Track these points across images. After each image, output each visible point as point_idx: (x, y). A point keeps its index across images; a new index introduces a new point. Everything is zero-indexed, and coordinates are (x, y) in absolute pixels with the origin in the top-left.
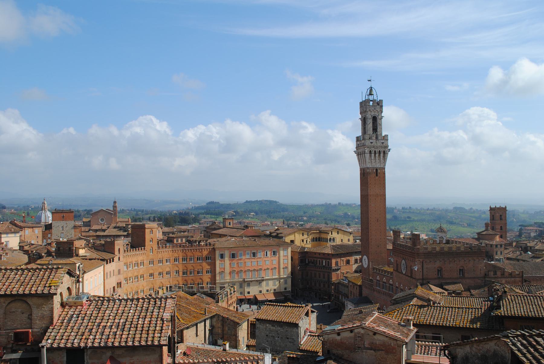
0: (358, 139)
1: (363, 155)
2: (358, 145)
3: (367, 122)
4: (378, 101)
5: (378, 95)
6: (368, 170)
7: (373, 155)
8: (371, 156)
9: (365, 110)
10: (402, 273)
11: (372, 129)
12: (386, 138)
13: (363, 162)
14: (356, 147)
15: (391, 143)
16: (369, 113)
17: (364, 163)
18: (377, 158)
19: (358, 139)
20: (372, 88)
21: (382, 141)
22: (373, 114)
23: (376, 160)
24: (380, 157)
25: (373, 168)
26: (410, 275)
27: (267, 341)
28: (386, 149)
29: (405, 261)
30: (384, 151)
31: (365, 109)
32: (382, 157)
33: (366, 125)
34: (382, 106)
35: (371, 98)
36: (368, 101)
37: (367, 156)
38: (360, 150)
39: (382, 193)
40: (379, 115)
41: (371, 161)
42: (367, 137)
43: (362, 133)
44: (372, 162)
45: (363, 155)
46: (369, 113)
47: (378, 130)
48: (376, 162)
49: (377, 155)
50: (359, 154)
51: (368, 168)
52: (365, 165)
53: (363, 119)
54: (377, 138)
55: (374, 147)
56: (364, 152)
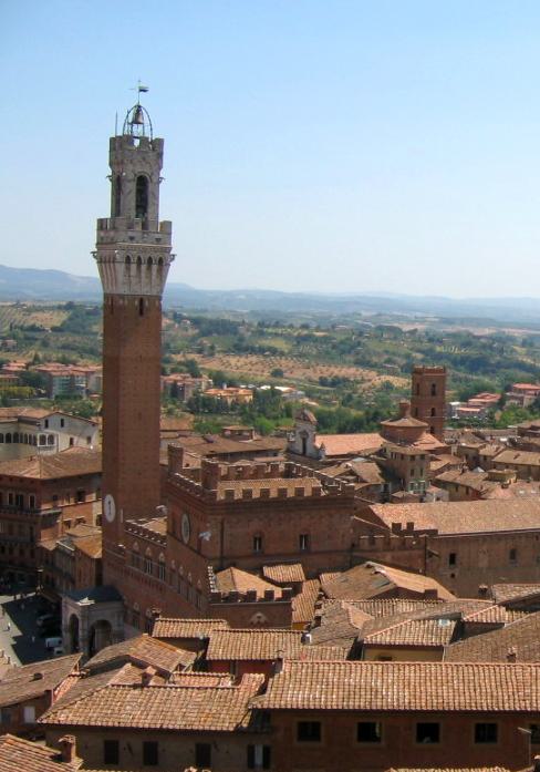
0: (102, 224)
2: (102, 238)
5: (154, 128)
7: (134, 267)
8: (128, 269)
11: (133, 204)
12: (167, 225)
14: (97, 244)
15: (178, 243)
16: (130, 167)
18: (143, 275)
20: (140, 107)
21: (157, 236)
22: (139, 169)
23: (140, 278)
24: (151, 274)
25: (134, 297)
26: (196, 548)
30: (160, 261)
31: (120, 158)
32: (154, 272)
34: (160, 155)
35: (137, 130)
36: (129, 139)
37: (121, 268)
38: (106, 253)
42: (121, 221)
49: (144, 267)
51: (122, 297)
54: (145, 226)
56: (114, 258)
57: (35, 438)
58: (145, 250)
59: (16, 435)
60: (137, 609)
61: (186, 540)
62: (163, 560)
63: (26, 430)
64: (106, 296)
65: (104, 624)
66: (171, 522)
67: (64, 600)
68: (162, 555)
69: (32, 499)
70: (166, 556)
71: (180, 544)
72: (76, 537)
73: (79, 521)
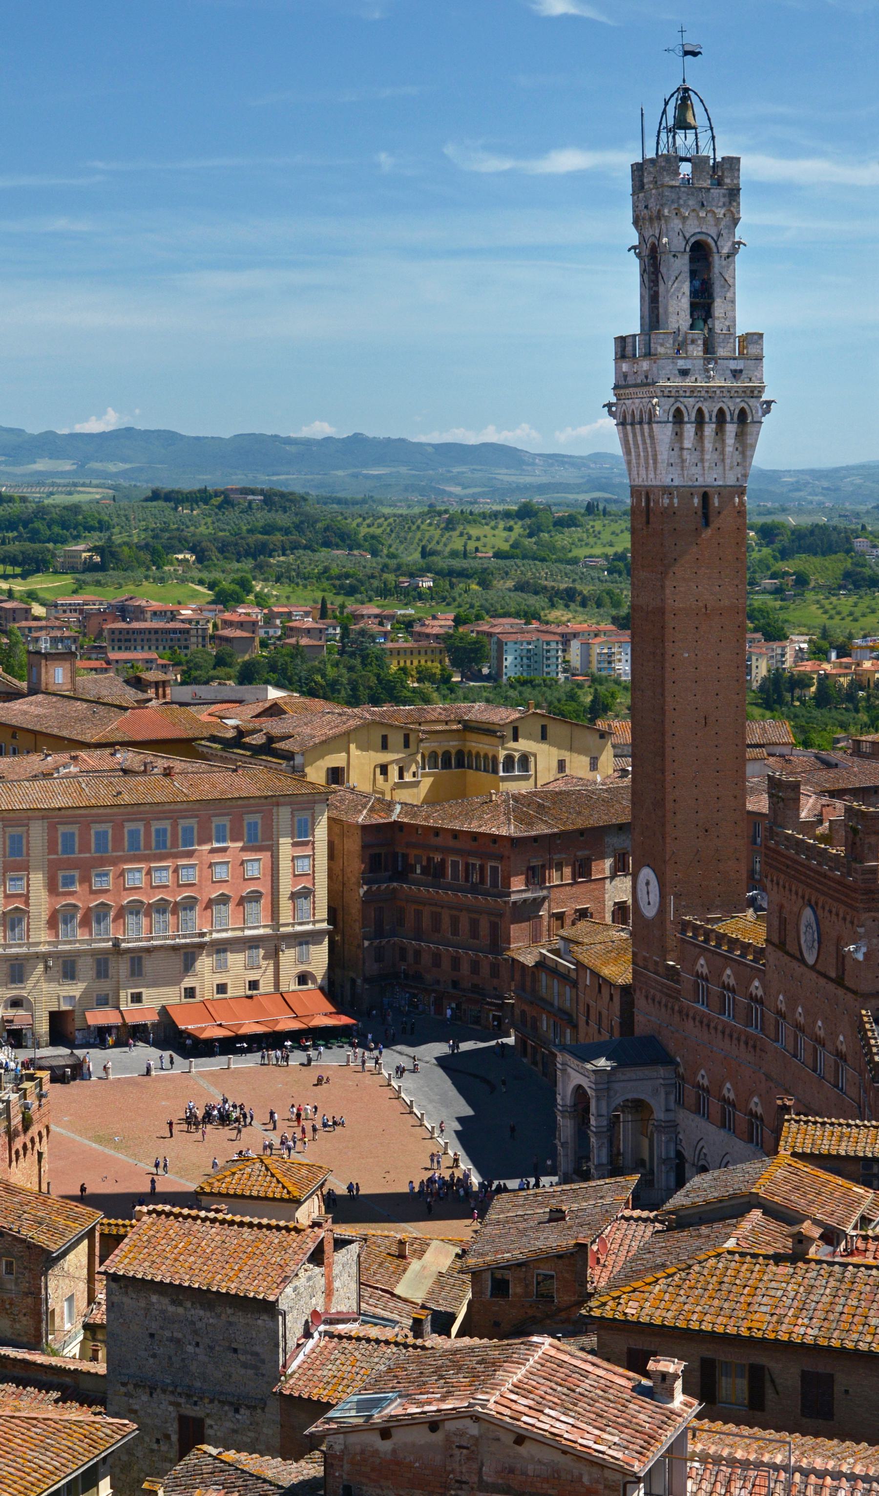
1: (646, 426)
2: (625, 376)
3: (663, 270)
4: (719, 159)
6: (666, 501)
7: (689, 430)
8: (678, 435)
9: (655, 213)
10: (802, 961)
13: (642, 461)
16: (676, 224)
17: (647, 462)
19: (624, 348)
21: (733, 365)
23: (702, 451)
24: (723, 441)
26: (833, 975)
27: (154, 1356)
28: (753, 402)
29: (815, 912)
32: (730, 439)
33: (661, 282)
37: (664, 433)
38: (634, 405)
39: (726, 602)
40: (719, 235)
41: (681, 456)
43: (642, 318)
44: (683, 461)
45: (646, 426)
46: (676, 224)
47: (719, 308)
48: (702, 460)
49: (709, 429)
50: (629, 420)
51: (667, 490)
52: (652, 476)
53: (646, 252)
54: (709, 348)
55: (693, 391)
56: (651, 414)
57: (495, 759)
58: (710, 394)
59: (460, 753)
60: (705, 1082)
61: (811, 959)
62: (760, 993)
63: (479, 745)
64: (635, 491)
65: (638, 1106)
66: (776, 922)
67: (559, 1059)
68: (756, 983)
69: (494, 869)
70: (764, 987)
71: (795, 964)
72: (577, 943)
73: (583, 914)
